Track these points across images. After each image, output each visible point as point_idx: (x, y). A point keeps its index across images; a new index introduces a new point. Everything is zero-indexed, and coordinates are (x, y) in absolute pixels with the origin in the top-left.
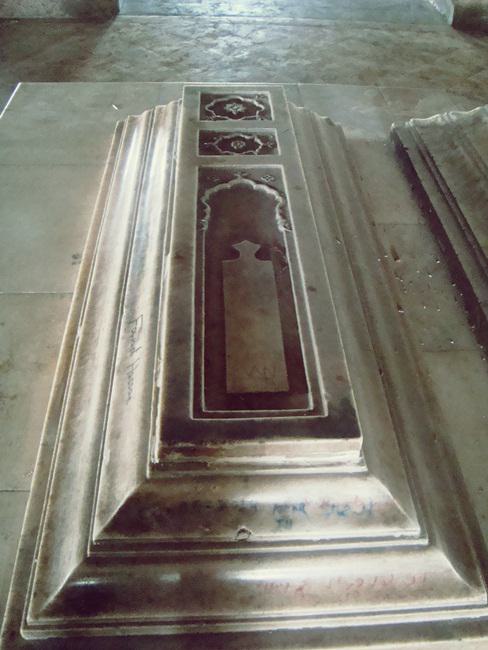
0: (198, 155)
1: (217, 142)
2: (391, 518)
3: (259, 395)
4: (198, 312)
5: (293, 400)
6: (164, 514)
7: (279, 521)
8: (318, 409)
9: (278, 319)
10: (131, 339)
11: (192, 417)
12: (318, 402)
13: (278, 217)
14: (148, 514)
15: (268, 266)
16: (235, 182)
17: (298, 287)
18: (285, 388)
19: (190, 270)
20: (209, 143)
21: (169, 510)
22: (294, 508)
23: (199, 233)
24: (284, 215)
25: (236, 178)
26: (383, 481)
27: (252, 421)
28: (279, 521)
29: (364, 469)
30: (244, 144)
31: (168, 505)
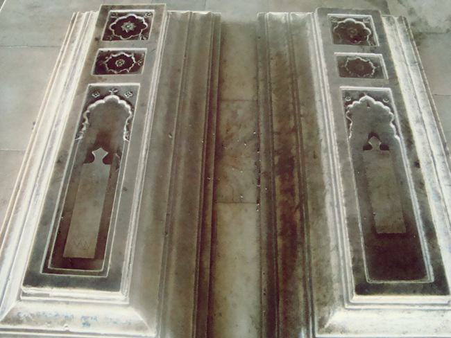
0: (92, 74)
1: (107, 61)
2: (140, 327)
3: (98, 245)
4: (61, 202)
5: (95, 263)
6: (31, 317)
7: (84, 324)
8: (104, 272)
9: (102, 207)
10: (34, 208)
11: (41, 272)
12: (106, 267)
13: (125, 129)
14: (22, 315)
15: (108, 168)
16: (108, 98)
17: (120, 185)
18: (92, 257)
19: (63, 172)
20: (104, 65)
21: (32, 315)
22: (92, 318)
23: (76, 142)
24: (128, 129)
25: (109, 94)
26: (136, 308)
27: (69, 277)
28: (84, 324)
29: (127, 303)
30: (124, 61)
31: (32, 312)
